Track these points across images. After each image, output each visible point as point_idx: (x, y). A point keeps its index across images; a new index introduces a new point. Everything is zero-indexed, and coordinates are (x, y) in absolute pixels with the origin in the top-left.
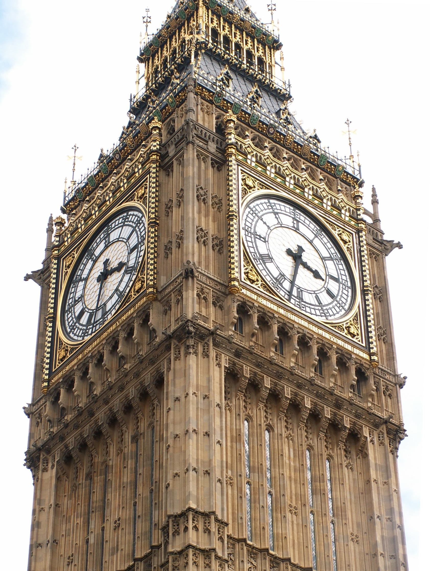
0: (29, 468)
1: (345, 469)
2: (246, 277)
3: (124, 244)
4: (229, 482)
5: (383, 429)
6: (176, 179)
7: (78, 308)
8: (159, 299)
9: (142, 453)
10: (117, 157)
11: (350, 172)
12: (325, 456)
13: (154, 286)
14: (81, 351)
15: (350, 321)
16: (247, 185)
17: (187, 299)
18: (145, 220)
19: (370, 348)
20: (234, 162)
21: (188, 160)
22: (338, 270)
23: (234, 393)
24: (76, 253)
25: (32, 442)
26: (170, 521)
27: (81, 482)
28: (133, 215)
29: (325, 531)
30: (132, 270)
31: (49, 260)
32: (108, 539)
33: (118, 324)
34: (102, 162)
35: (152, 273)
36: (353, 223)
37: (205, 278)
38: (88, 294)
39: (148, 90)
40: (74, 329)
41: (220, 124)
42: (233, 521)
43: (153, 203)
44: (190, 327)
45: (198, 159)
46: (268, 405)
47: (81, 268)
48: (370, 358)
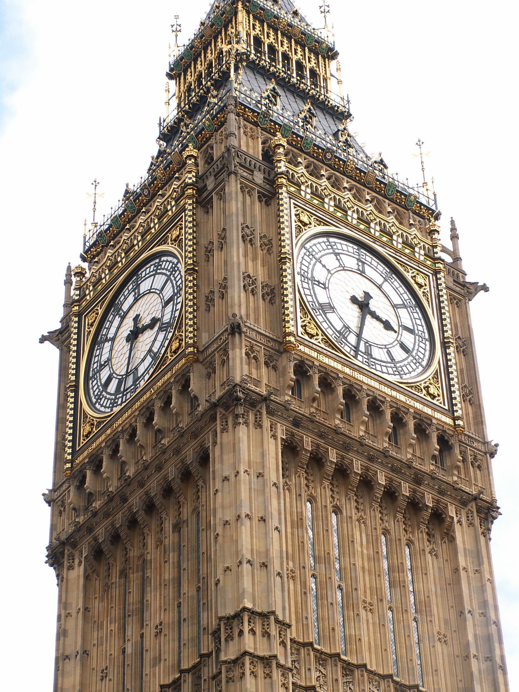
0: (51, 565)
1: (429, 556)
2: (303, 331)
3: (157, 296)
4: (290, 576)
5: (472, 507)
6: (217, 216)
7: (105, 374)
8: (201, 360)
9: (186, 544)
10: (146, 192)
11: (424, 202)
12: (404, 542)
13: (194, 345)
14: (110, 425)
15: (429, 380)
17: (234, 359)
18: (182, 267)
19: (453, 411)
20: (285, 194)
21: (230, 194)
22: (413, 320)
23: (293, 470)
24: (100, 309)
25: (55, 535)
26: (222, 623)
27: (113, 581)
28: (167, 261)
29: (406, 630)
30: (167, 327)
31: (68, 317)
32: (148, 648)
33: (153, 391)
34: (128, 199)
35: (191, 329)
36: (429, 263)
38: (115, 356)
39: (180, 111)
40: (101, 399)
41: (267, 150)
42: (297, 622)
43: (190, 246)
44: (238, 393)
45: (242, 192)
46: (335, 483)
47: (107, 326)
48: (455, 423)
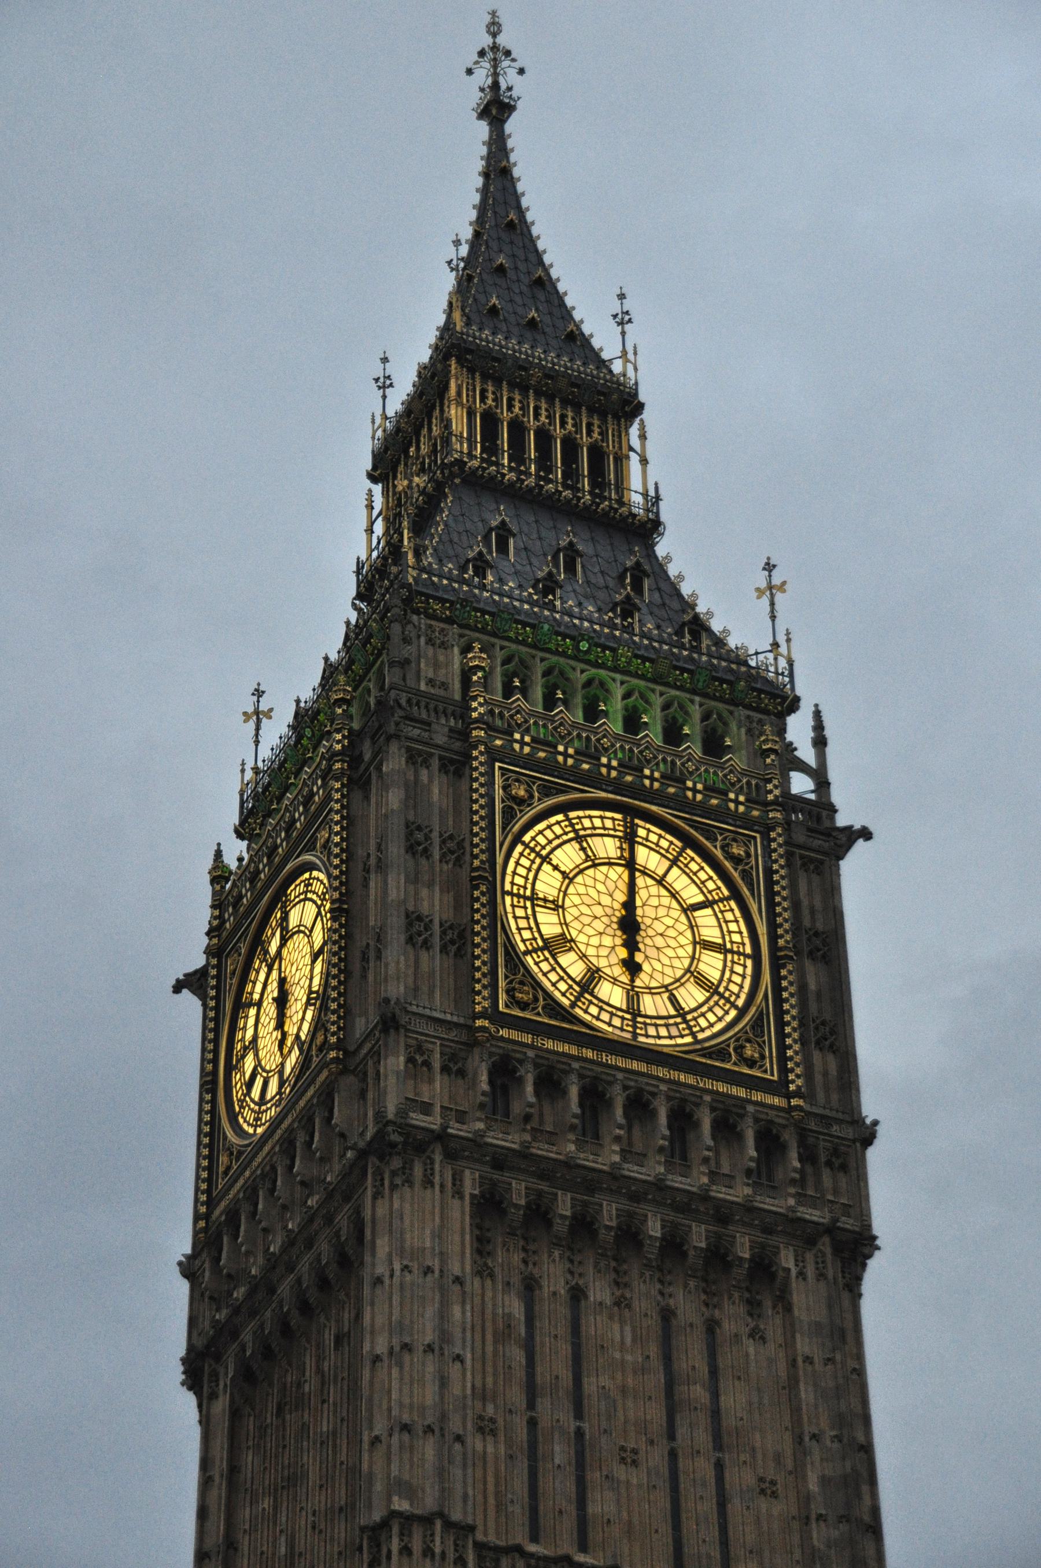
0: (190, 1389)
9: (345, 1374)
15: (746, 1032)
27: (269, 1421)
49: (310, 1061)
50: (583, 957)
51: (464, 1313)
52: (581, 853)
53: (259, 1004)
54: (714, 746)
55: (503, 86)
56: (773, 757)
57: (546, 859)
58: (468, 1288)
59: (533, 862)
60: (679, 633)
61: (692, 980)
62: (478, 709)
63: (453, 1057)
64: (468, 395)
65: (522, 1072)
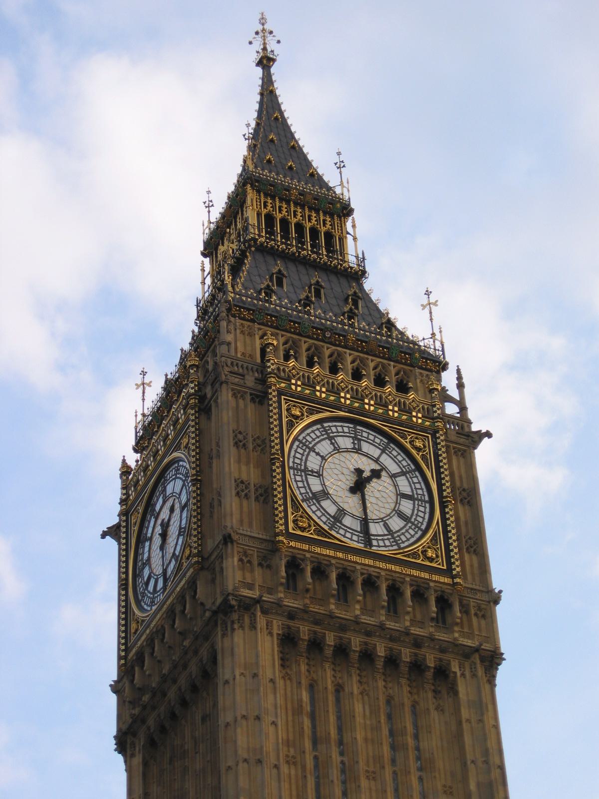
0: (119, 753)
8: (206, 567)
16: (293, 416)
37: (247, 538)
40: (144, 597)
48: (453, 581)
49: (182, 565)
50: (335, 503)
51: (275, 698)
52: (331, 445)
53: (151, 539)
54: (402, 388)
55: (269, 50)
56: (436, 393)
57: (312, 449)
58: (278, 685)
59: (305, 451)
60: (380, 327)
61: (396, 515)
62: (271, 367)
63: (265, 558)
64: (257, 205)
65: (303, 566)
